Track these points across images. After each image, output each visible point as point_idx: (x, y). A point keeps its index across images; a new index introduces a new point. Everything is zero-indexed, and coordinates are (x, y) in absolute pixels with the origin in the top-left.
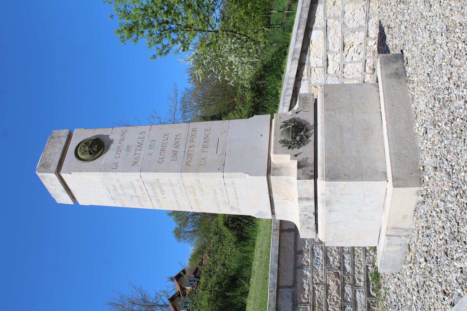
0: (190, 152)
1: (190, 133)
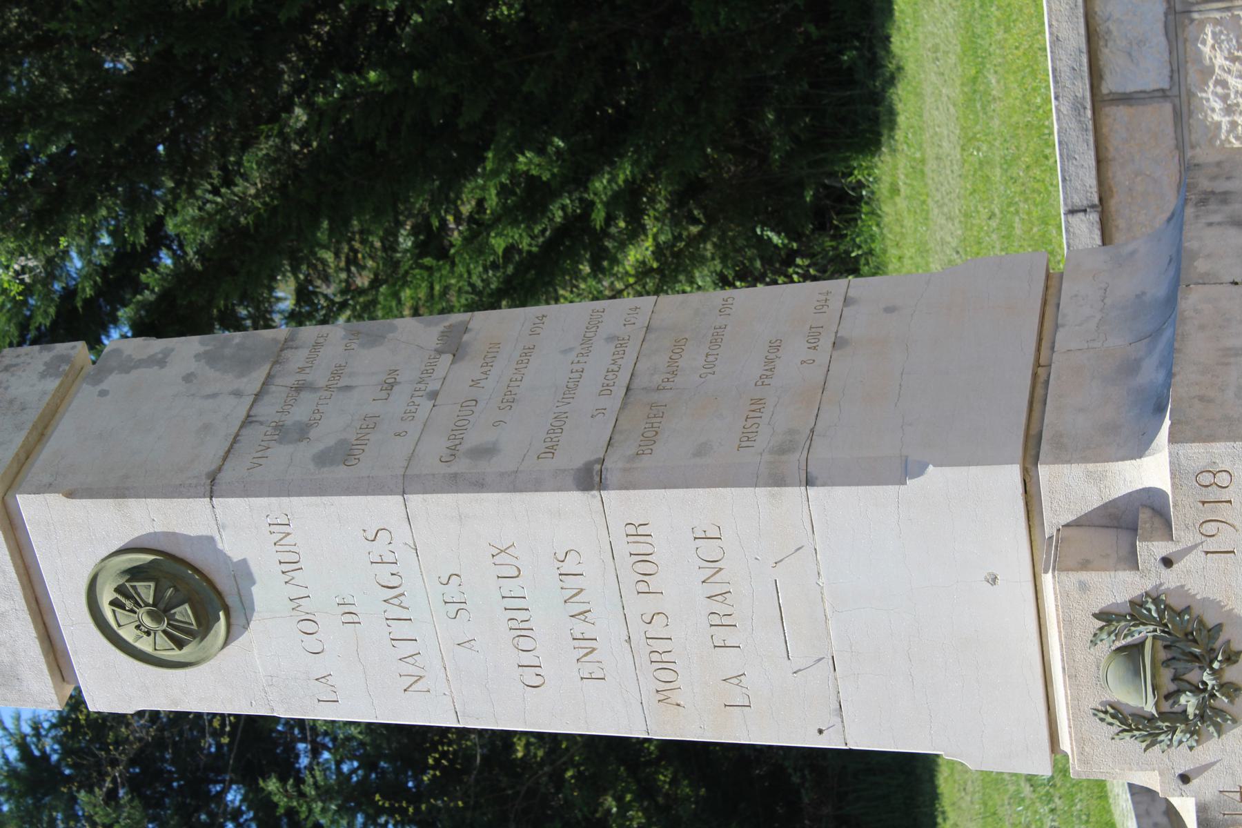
0: (660, 646)
1: (622, 548)
